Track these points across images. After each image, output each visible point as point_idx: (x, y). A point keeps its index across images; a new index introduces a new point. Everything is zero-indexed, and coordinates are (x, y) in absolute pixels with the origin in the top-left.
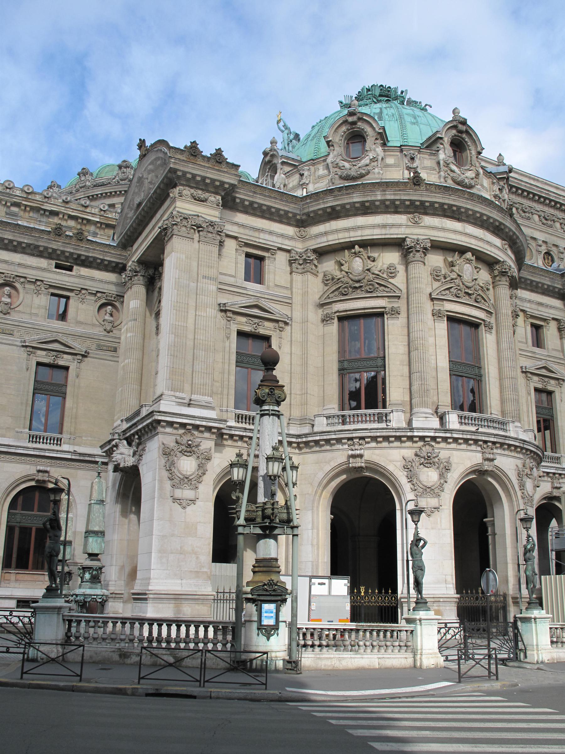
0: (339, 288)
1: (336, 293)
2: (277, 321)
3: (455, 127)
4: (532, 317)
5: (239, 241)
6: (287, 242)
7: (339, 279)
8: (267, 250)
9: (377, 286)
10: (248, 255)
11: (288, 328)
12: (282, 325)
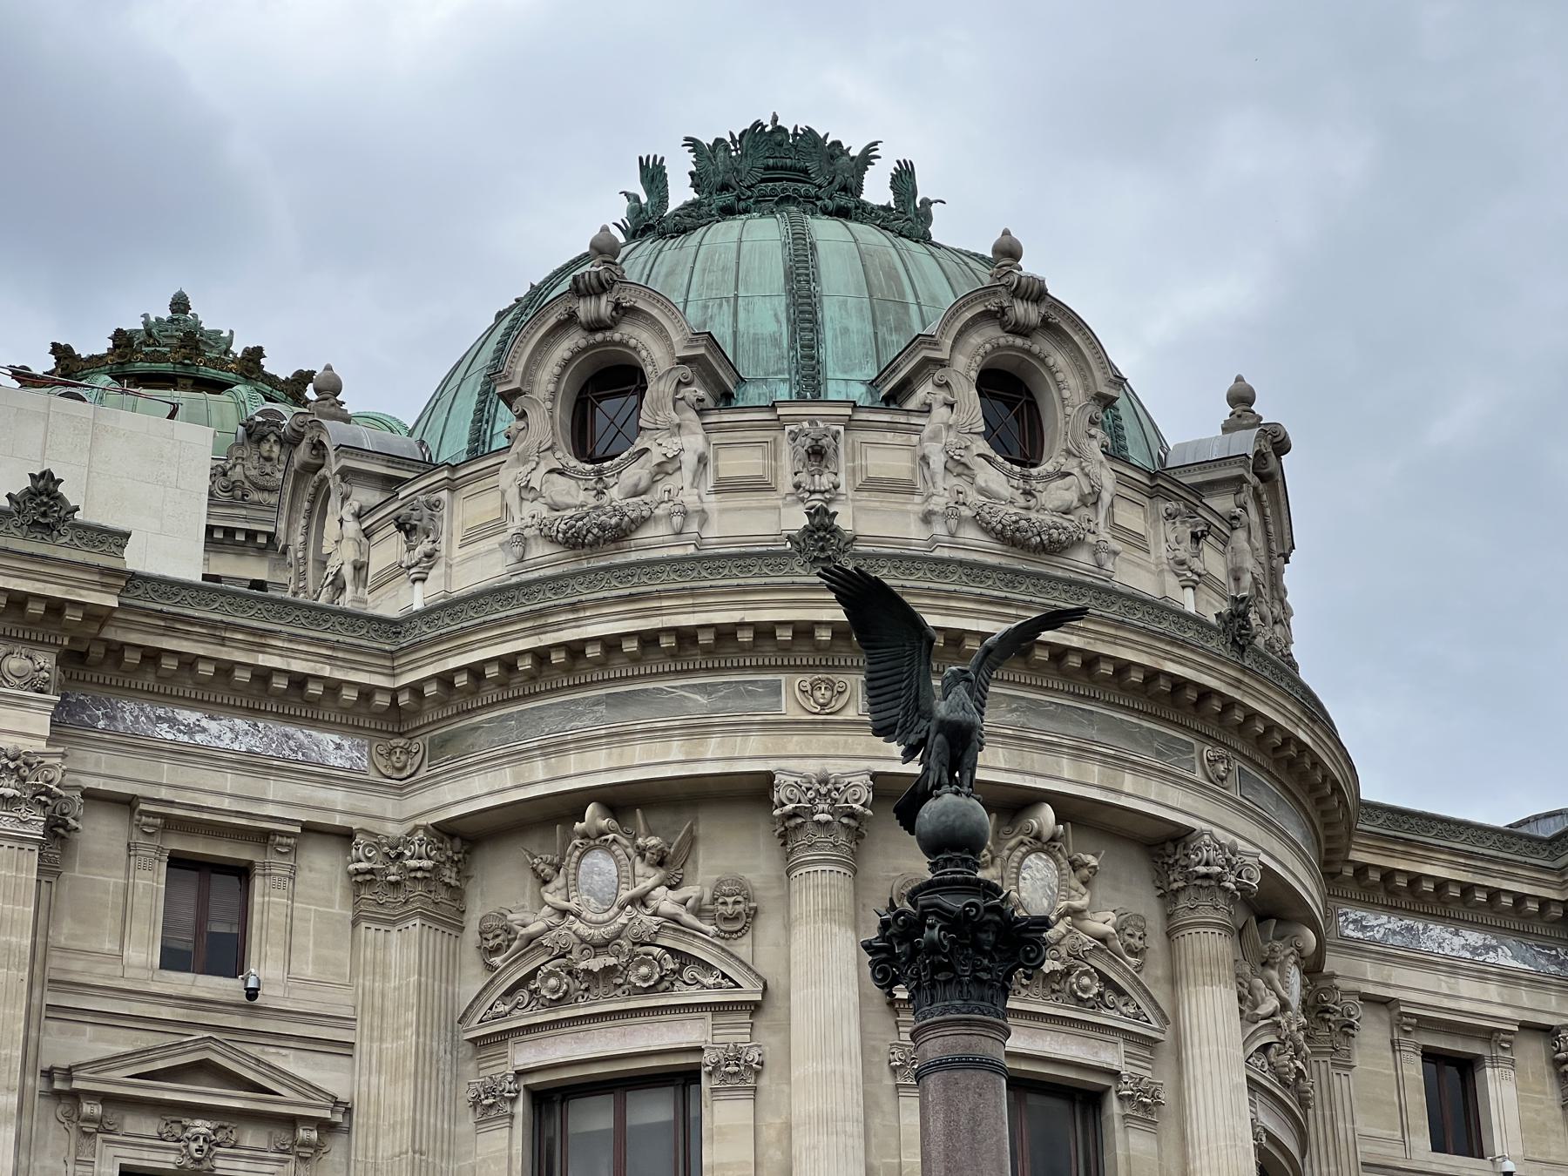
0: (532, 975)
1: (523, 995)
2: (292, 1122)
3: (995, 316)
4: (1425, 1024)
5: (142, 813)
6: (338, 797)
7: (530, 939)
8: (263, 838)
10: (178, 862)
11: (336, 1145)
12: (307, 1134)
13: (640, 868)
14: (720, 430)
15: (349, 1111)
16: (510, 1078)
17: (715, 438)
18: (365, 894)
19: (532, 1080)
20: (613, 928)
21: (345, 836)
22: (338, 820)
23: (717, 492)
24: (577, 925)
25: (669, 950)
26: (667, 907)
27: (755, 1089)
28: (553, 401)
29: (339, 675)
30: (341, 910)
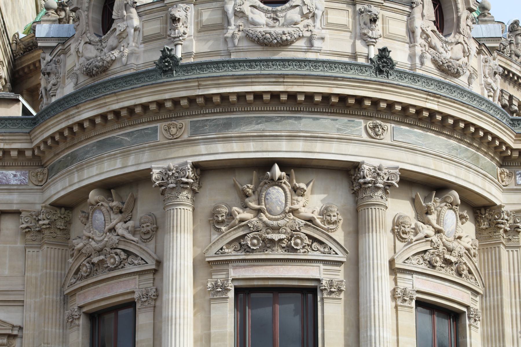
7: (79, 250)
9: (123, 256)
13: (113, 216)
14: (146, 14)
15: (21, 328)
16: (76, 310)
17: (144, 18)
18: (28, 237)
19: (85, 310)
20: (103, 242)
21: (17, 213)
22: (15, 207)
23: (144, 43)
24: (93, 243)
25: (124, 250)
26: (120, 231)
27: (155, 307)
28: (88, 11)
29: (7, 147)
30: (20, 245)
